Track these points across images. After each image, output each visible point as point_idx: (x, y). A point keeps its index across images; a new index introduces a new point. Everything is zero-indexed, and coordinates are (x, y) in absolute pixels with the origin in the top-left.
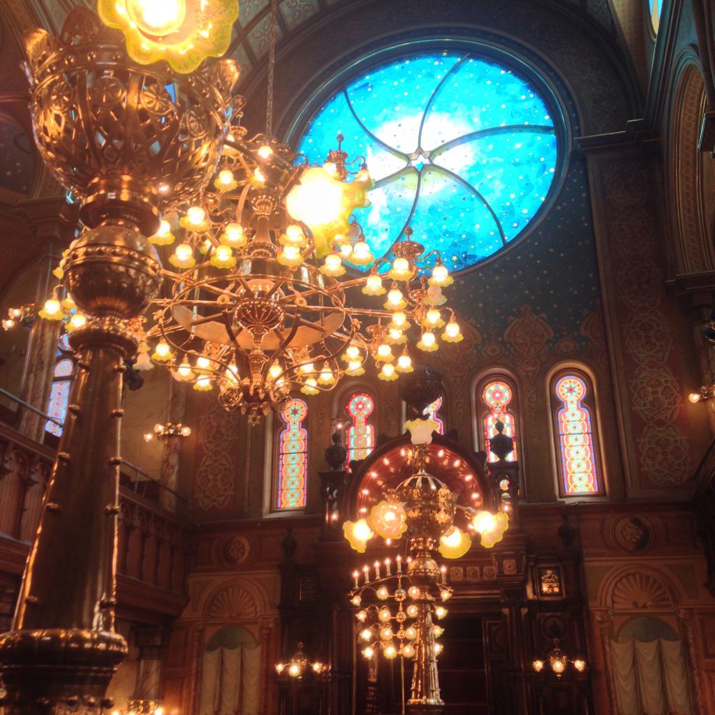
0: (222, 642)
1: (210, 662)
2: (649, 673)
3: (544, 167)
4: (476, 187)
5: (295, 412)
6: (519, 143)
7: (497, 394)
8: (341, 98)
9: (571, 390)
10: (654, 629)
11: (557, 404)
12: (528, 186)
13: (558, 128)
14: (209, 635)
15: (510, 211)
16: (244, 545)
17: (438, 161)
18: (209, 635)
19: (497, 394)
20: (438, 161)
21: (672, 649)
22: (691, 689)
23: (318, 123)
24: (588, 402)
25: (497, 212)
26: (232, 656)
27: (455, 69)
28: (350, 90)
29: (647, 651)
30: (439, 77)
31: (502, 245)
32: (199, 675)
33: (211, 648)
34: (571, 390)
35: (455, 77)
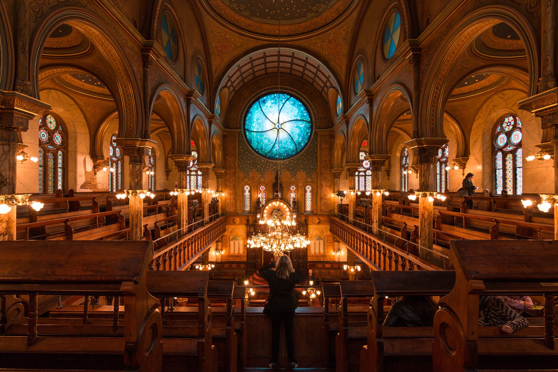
0: (234, 239)
1: (232, 243)
2: (317, 246)
3: (308, 133)
6: (302, 125)
7: (293, 188)
8: (257, 103)
9: (309, 188)
10: (319, 238)
11: (305, 191)
12: (303, 138)
13: (311, 122)
14: (231, 237)
15: (299, 143)
16: (238, 220)
17: (282, 126)
18: (231, 237)
19: (293, 188)
20: (282, 126)
21: (322, 242)
22: (324, 248)
23: (252, 110)
24: (311, 192)
26: (236, 242)
27: (288, 100)
28: (260, 100)
29: (317, 242)
30: (284, 101)
32: (230, 245)
33: (232, 240)
34: (309, 188)
35: (287, 102)
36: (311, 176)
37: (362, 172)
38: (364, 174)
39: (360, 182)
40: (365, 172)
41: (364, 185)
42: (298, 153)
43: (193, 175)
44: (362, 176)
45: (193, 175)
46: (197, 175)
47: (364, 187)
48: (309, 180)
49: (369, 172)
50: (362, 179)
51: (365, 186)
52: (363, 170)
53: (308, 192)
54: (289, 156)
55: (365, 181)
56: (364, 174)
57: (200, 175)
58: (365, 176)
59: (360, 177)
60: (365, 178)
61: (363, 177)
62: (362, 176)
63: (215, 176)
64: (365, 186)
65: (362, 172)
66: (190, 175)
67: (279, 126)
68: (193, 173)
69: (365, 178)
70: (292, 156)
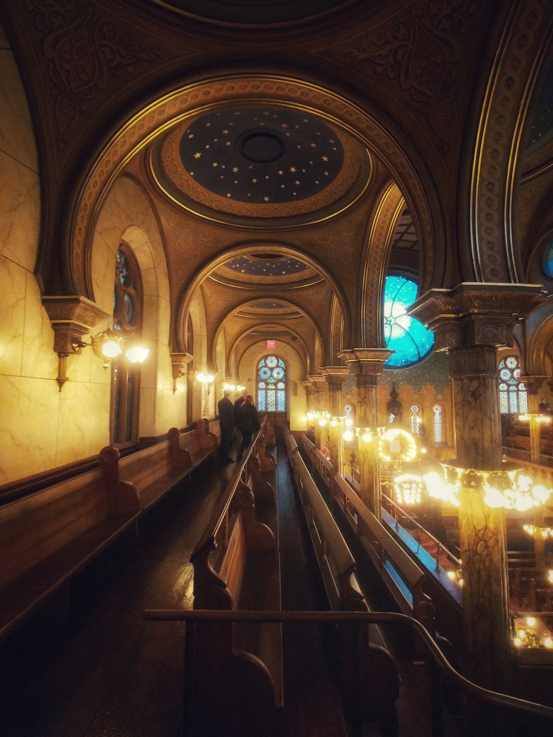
4: (411, 335)
5: (348, 409)
11: (434, 414)
15: (423, 345)
17: (398, 321)
25: (418, 344)
31: (418, 359)
35: (404, 288)
36: (443, 391)
41: (516, 404)
42: (421, 359)
43: (272, 389)
44: (514, 391)
45: (272, 389)
46: (276, 389)
47: (516, 408)
48: (440, 397)
50: (513, 395)
51: (518, 406)
54: (409, 364)
57: (281, 390)
58: (518, 391)
59: (511, 393)
60: (518, 395)
61: (515, 393)
62: (514, 391)
63: (304, 391)
64: (518, 406)
65: (512, 385)
66: (266, 389)
67: (391, 321)
68: (271, 387)
69: (518, 395)
70: (413, 363)
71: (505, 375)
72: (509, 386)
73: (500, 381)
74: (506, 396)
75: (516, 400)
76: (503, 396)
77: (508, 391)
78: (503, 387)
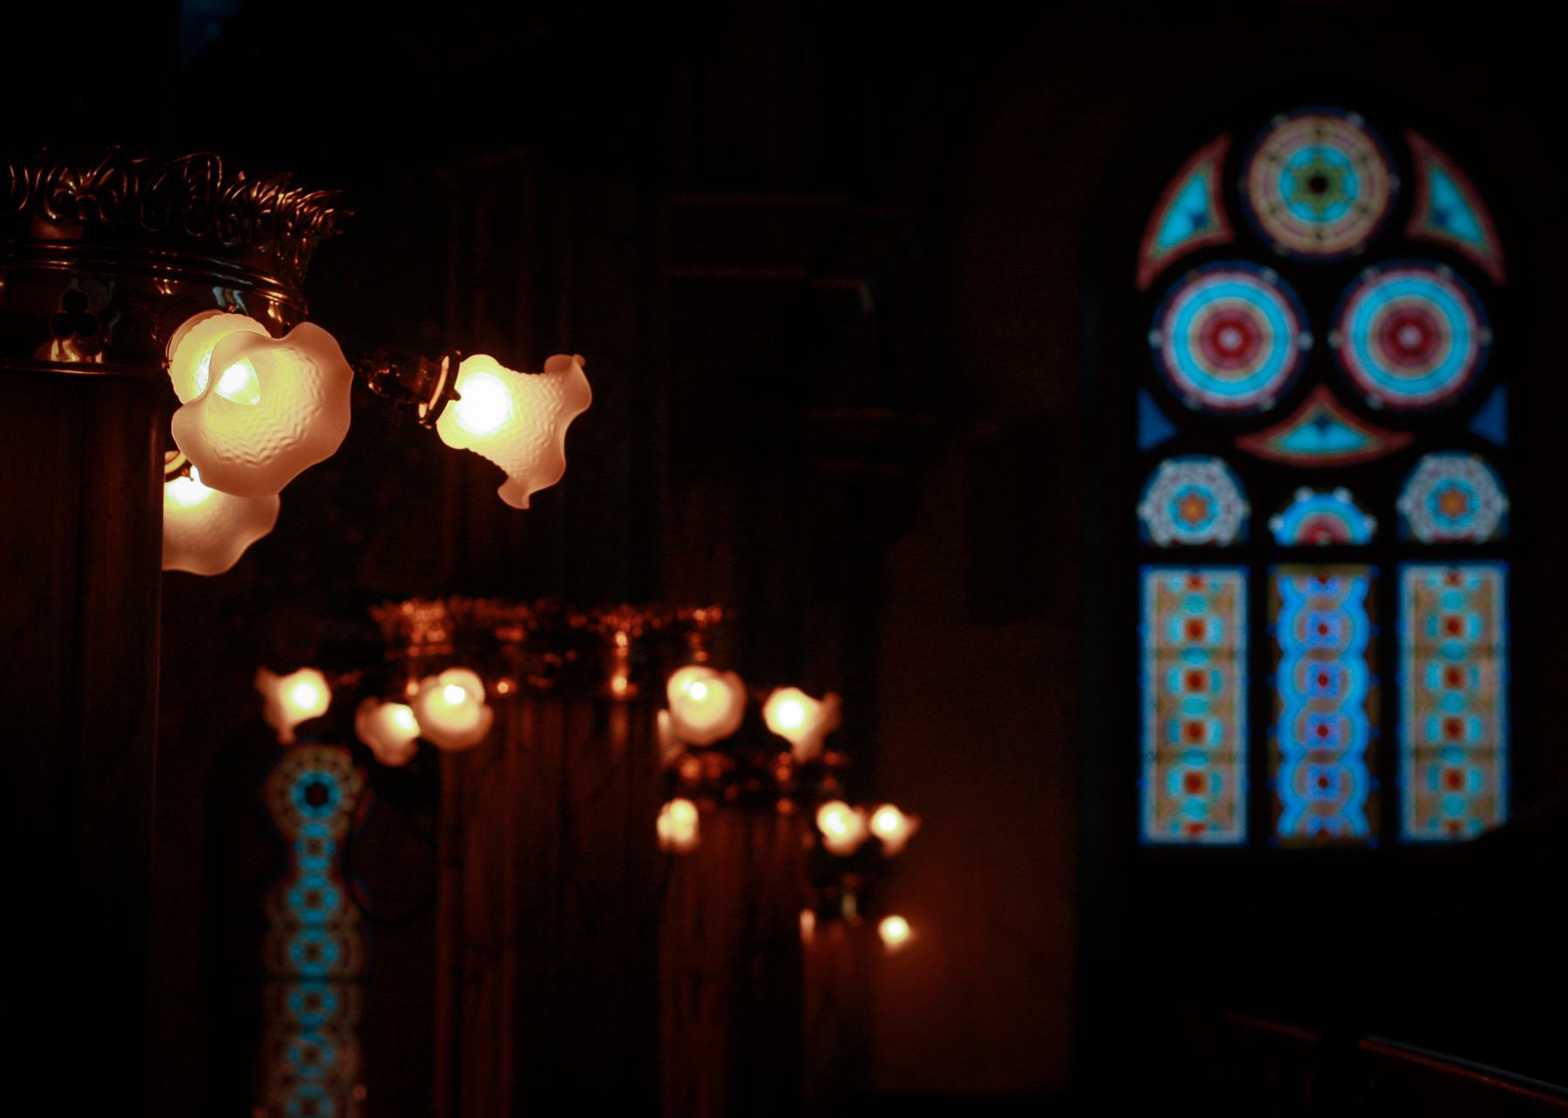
37: (1322, 475)
38: (1359, 528)
39: (1293, 679)
40: (1376, 484)
44: (1321, 555)
49: (1457, 494)
50: (1323, 615)
52: (1343, 439)
53: (314, 870)
55: (1384, 655)
56: (1359, 528)
58: (1390, 553)
60: (1383, 608)
61: (1349, 590)
62: (1321, 555)
65: (1322, 475)
69: (1383, 608)
71: (1217, 339)
72: (1268, 485)
73: (1153, 428)
74: (1226, 627)
75: (1355, 678)
76: (1187, 625)
77: (1255, 555)
78: (1190, 499)
